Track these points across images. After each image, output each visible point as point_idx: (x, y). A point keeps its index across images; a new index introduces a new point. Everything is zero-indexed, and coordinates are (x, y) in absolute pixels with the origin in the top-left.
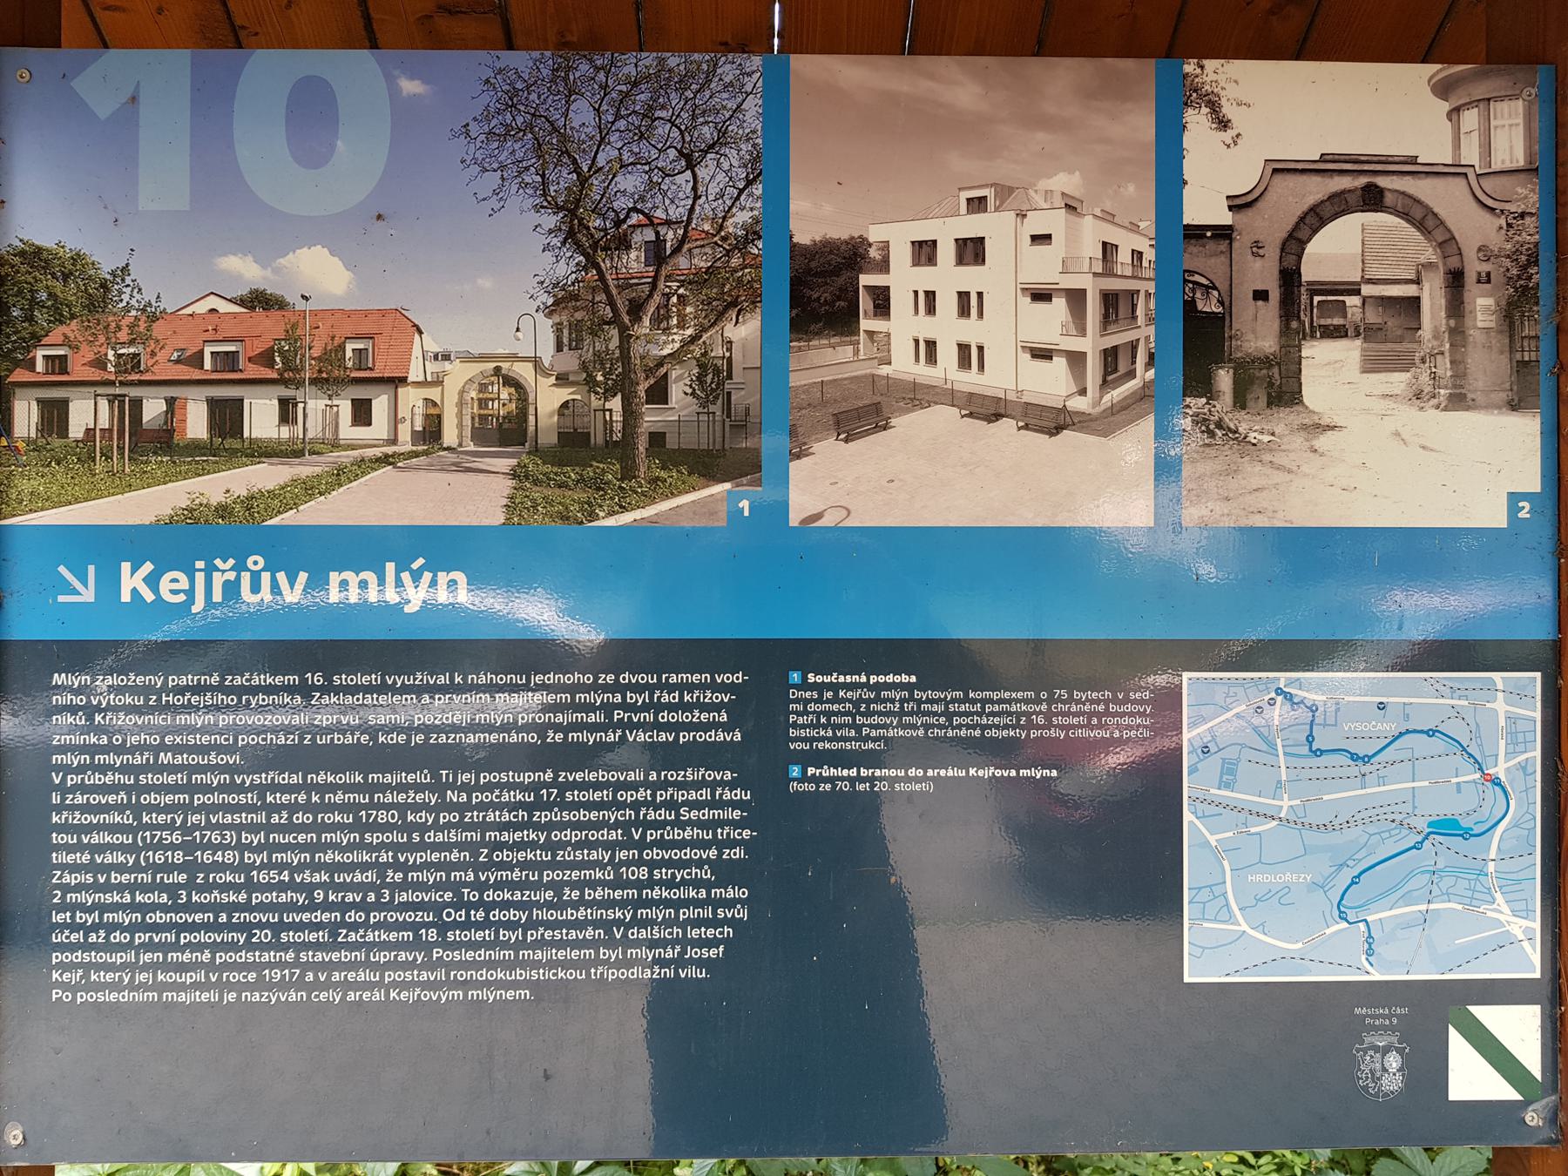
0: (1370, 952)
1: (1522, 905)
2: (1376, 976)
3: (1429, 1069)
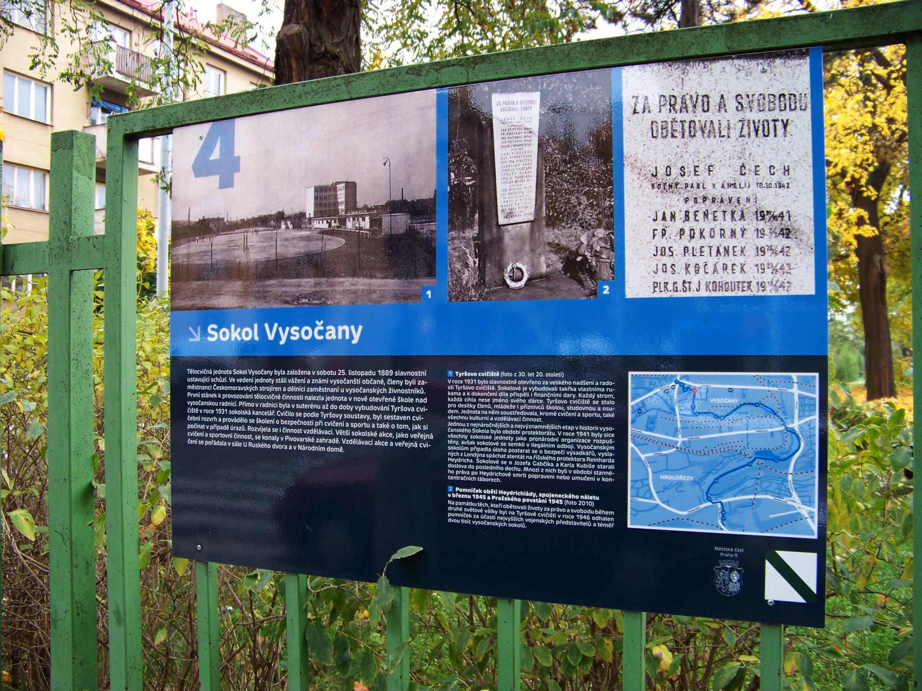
0: (723, 519)
1: (807, 499)
2: (726, 531)
3: (755, 581)
